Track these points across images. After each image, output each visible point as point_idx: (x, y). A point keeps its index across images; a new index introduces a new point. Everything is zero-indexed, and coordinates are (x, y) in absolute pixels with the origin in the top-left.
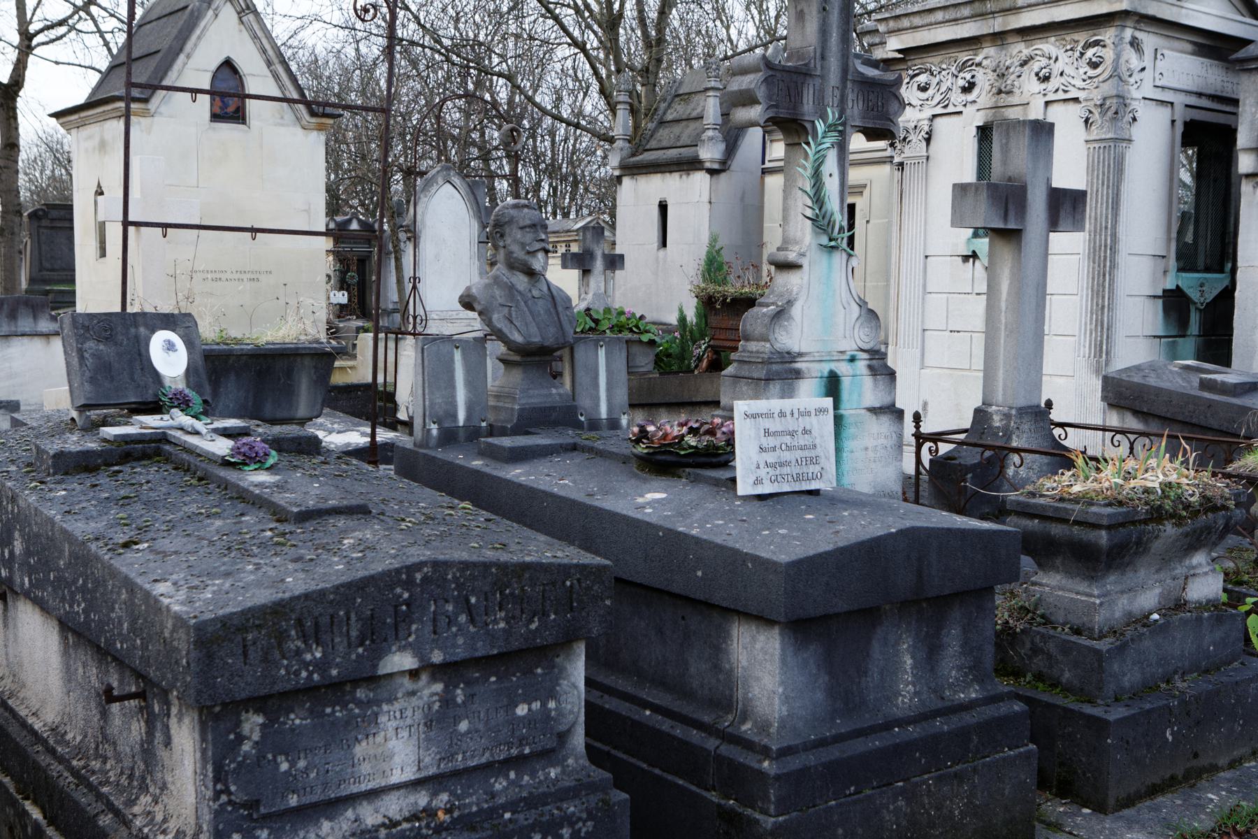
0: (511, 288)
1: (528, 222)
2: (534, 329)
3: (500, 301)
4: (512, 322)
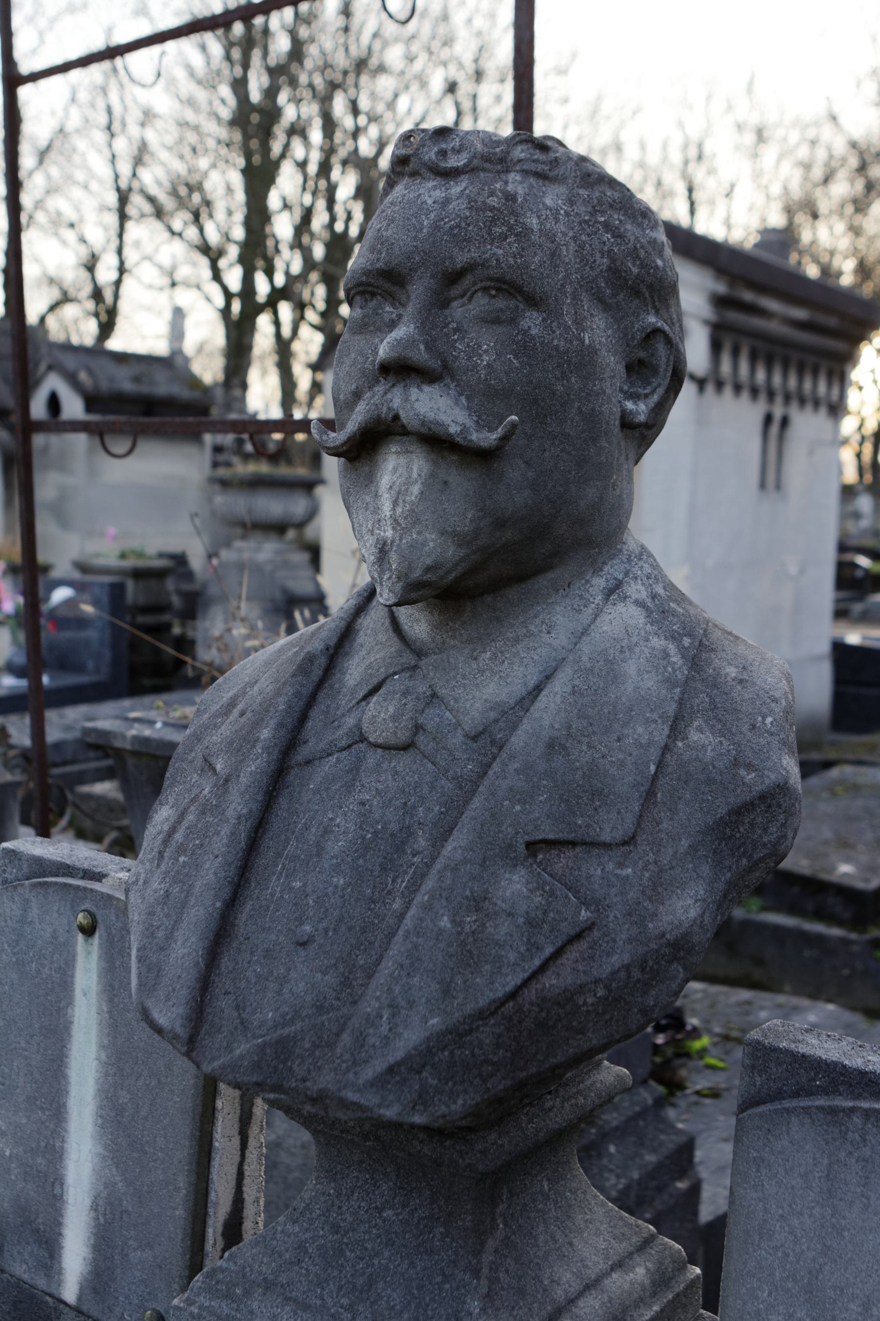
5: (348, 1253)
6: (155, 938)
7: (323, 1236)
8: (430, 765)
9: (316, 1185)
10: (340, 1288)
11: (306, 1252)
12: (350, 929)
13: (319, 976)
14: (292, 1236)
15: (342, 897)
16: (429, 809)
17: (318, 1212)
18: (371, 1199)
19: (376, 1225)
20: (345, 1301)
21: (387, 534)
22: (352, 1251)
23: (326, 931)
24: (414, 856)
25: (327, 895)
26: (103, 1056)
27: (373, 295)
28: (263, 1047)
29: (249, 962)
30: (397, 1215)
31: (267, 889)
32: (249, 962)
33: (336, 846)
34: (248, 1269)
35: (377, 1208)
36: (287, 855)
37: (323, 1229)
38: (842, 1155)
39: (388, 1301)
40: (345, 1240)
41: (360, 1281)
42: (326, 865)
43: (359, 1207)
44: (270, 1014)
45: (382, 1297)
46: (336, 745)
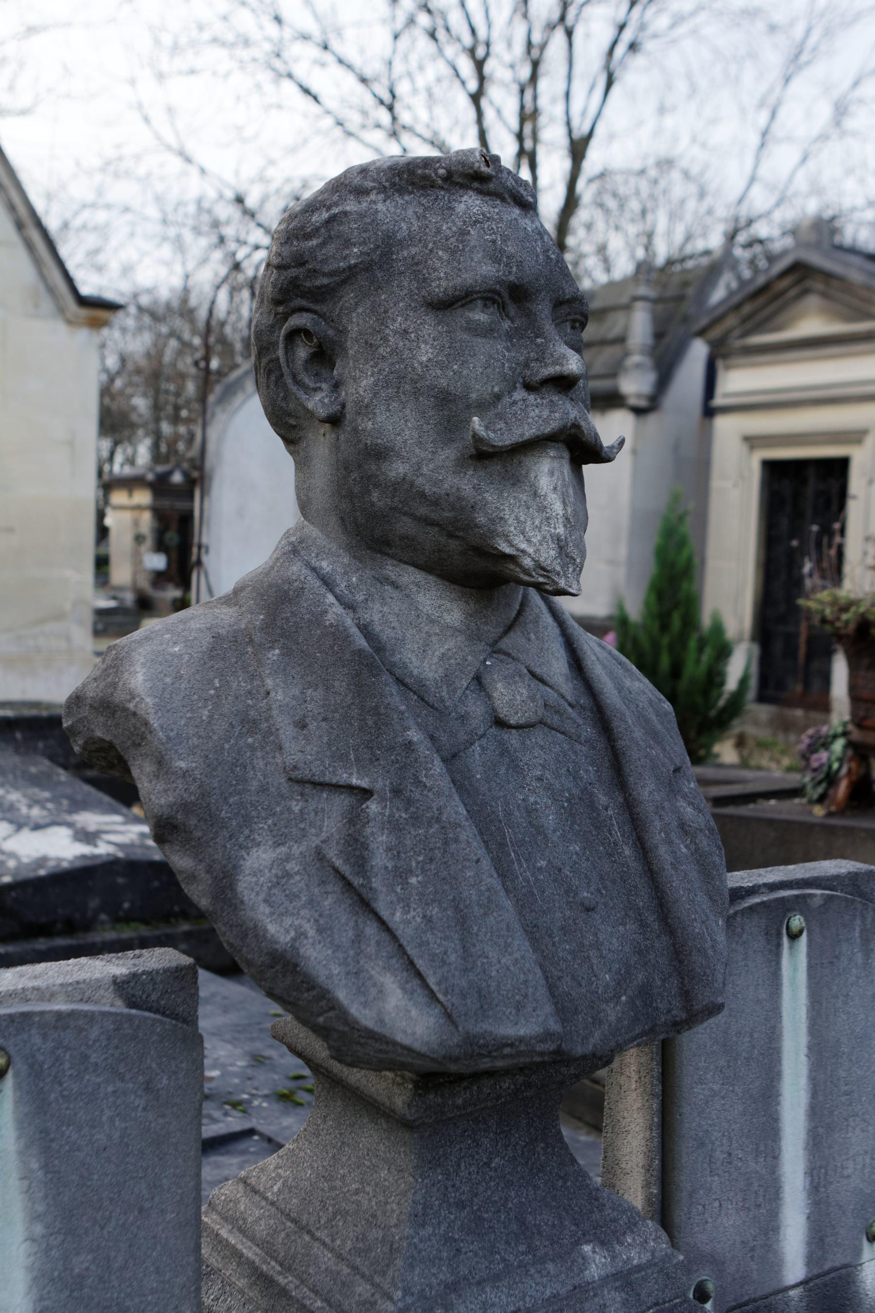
0: (372, 663)
1: (482, 270)
2: (508, 957)
3: (299, 751)
4: (363, 904)
5: (486, 1216)
6: (450, 964)
7: (456, 1218)
8: (559, 735)
9: (423, 1181)
10: (508, 1243)
11: (455, 1240)
12: (614, 882)
13: (621, 928)
14: (432, 1238)
15: (588, 860)
16: (587, 771)
17: (437, 1202)
18: (477, 1160)
19: (491, 1178)
20: (522, 1248)
21: (557, 531)
22: (487, 1212)
23: (599, 891)
24: (606, 810)
25: (575, 863)
26: (39, 1229)
27: (494, 302)
28: (631, 1001)
29: (554, 944)
30: (504, 1158)
31: (517, 877)
32: (554, 944)
33: (550, 820)
34: (427, 1289)
35: (485, 1164)
36: (511, 842)
37: (450, 1213)
38: (734, 945)
39: (546, 1224)
40: (475, 1208)
41: (514, 1227)
42: (555, 839)
43: (470, 1174)
44: (607, 976)
45: (540, 1225)
46: (476, 734)
